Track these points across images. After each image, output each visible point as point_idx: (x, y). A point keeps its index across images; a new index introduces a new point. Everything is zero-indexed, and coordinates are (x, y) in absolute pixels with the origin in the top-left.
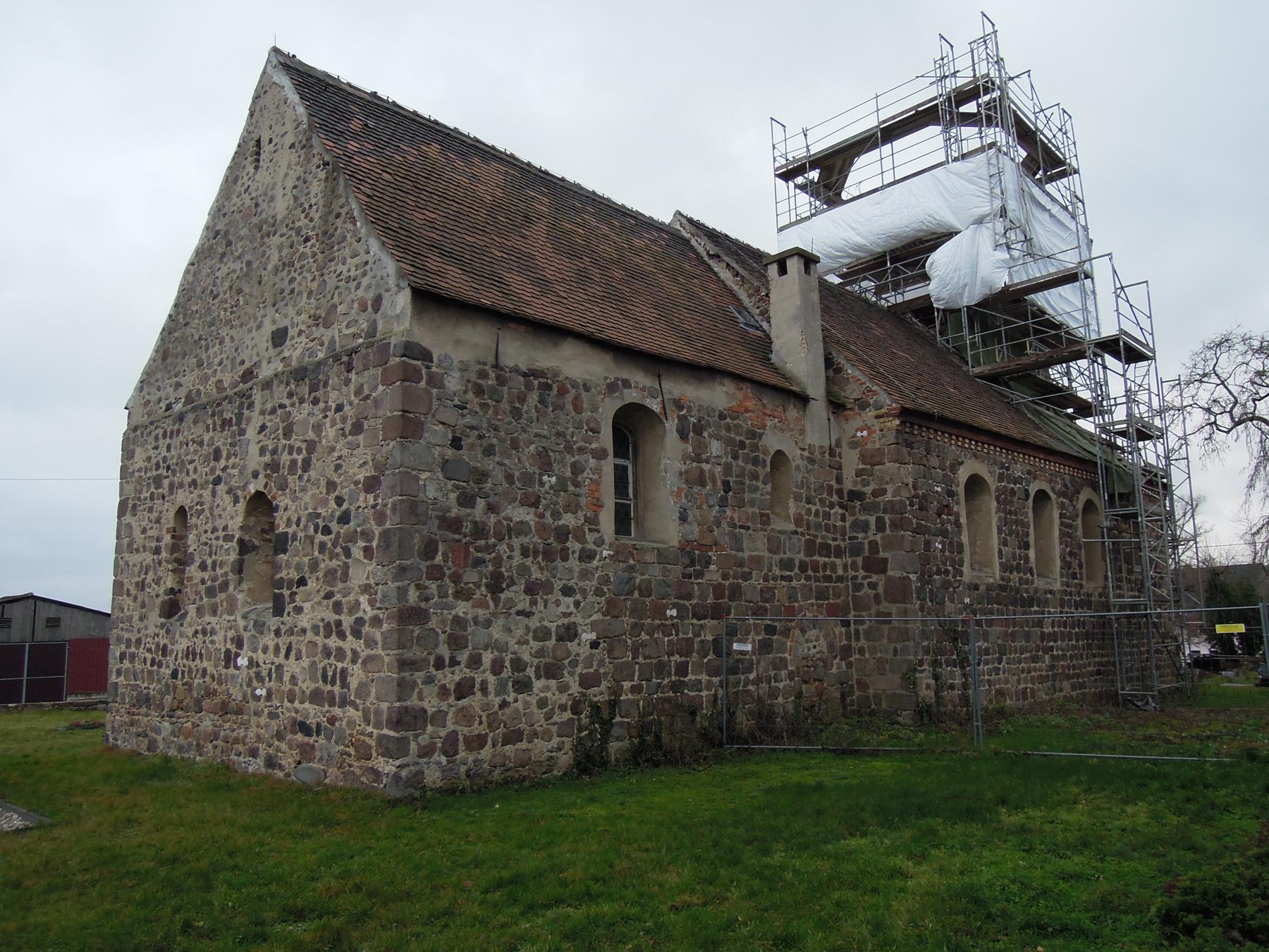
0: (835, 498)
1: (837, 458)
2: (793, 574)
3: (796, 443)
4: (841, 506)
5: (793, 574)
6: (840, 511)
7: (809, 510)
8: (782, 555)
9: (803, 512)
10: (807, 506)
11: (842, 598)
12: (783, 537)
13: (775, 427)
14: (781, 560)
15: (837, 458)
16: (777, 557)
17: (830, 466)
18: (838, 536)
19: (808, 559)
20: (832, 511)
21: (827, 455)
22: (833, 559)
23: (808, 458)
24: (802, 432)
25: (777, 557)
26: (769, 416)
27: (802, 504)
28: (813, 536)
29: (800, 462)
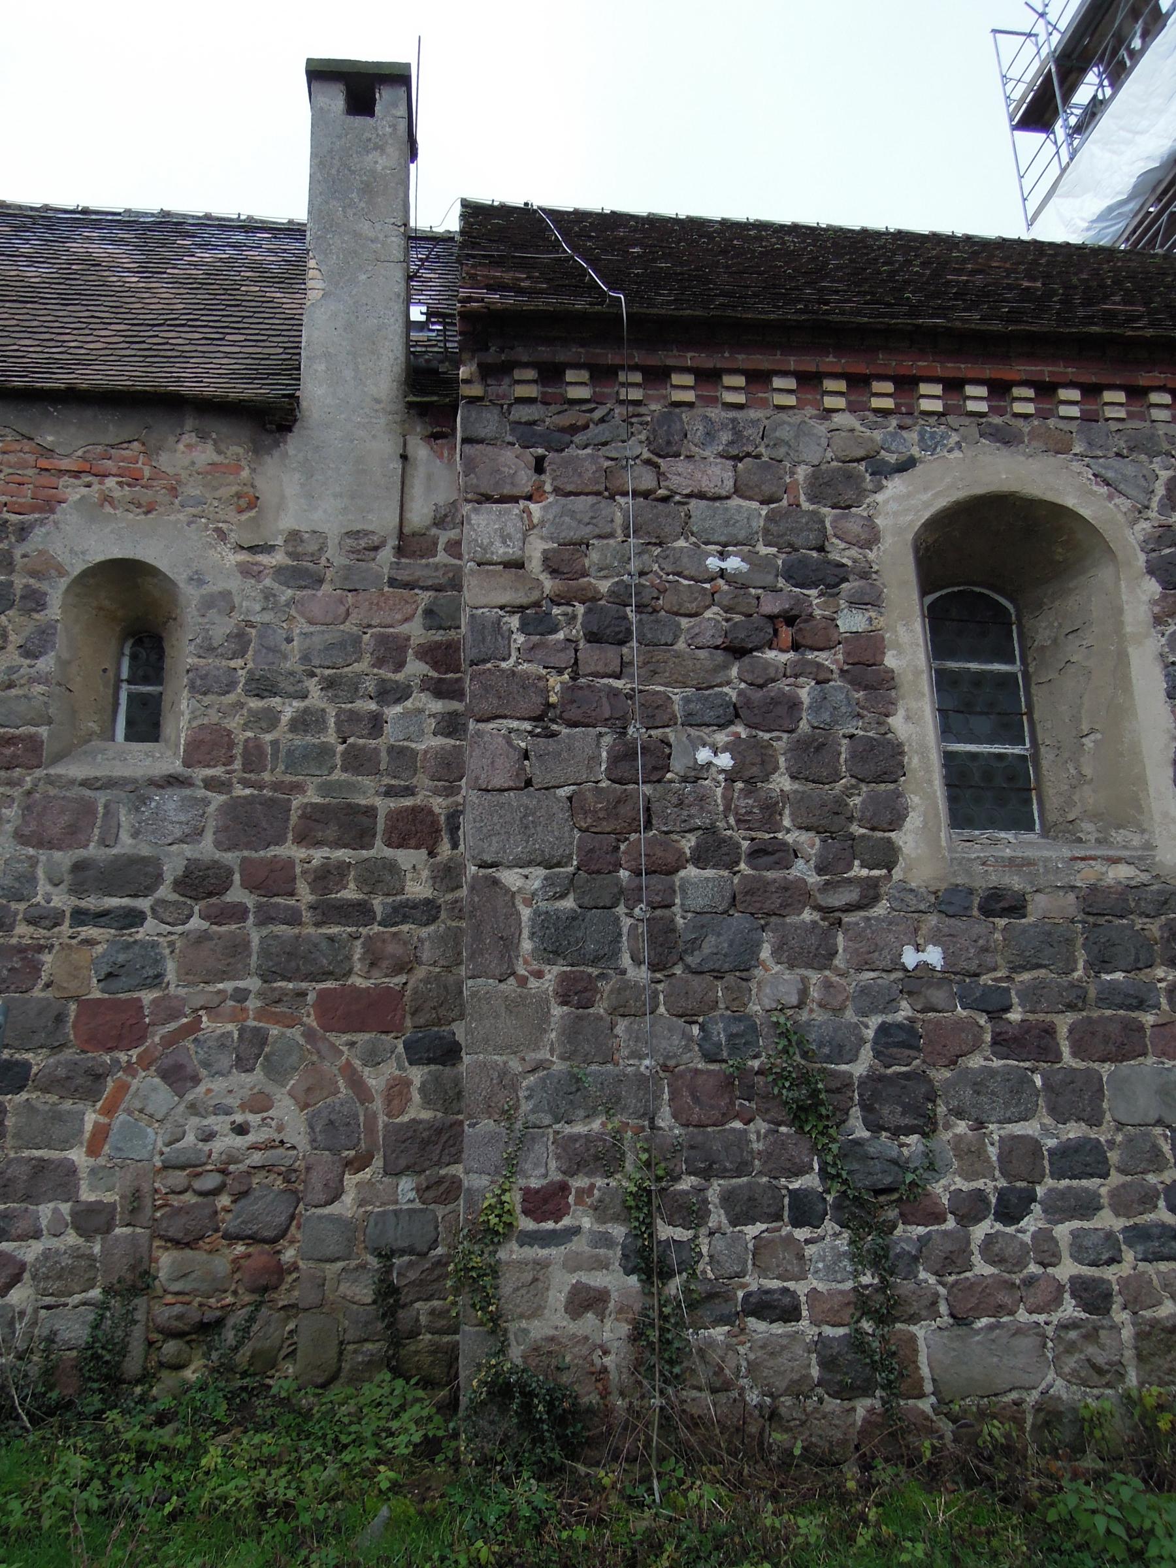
0: (415, 668)
1: (442, 557)
2: (144, 904)
3: (222, 535)
4: (440, 690)
5: (144, 904)
6: (437, 706)
7: (270, 719)
8: (92, 851)
9: (233, 723)
10: (255, 704)
11: (421, 972)
12: (102, 798)
13: (107, 499)
14: (79, 867)
15: (442, 557)
16: (64, 858)
17: (392, 582)
18: (422, 781)
19: (230, 858)
20: (393, 711)
21: (386, 555)
22: (380, 850)
23: (279, 571)
24: (250, 502)
25: (64, 858)
26: (76, 474)
27: (231, 698)
28: (276, 786)
29: (234, 584)
